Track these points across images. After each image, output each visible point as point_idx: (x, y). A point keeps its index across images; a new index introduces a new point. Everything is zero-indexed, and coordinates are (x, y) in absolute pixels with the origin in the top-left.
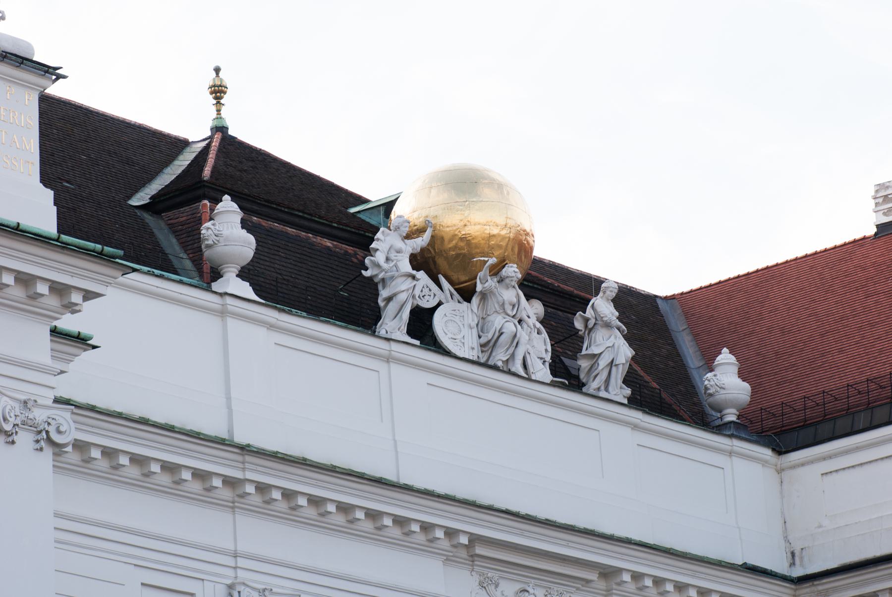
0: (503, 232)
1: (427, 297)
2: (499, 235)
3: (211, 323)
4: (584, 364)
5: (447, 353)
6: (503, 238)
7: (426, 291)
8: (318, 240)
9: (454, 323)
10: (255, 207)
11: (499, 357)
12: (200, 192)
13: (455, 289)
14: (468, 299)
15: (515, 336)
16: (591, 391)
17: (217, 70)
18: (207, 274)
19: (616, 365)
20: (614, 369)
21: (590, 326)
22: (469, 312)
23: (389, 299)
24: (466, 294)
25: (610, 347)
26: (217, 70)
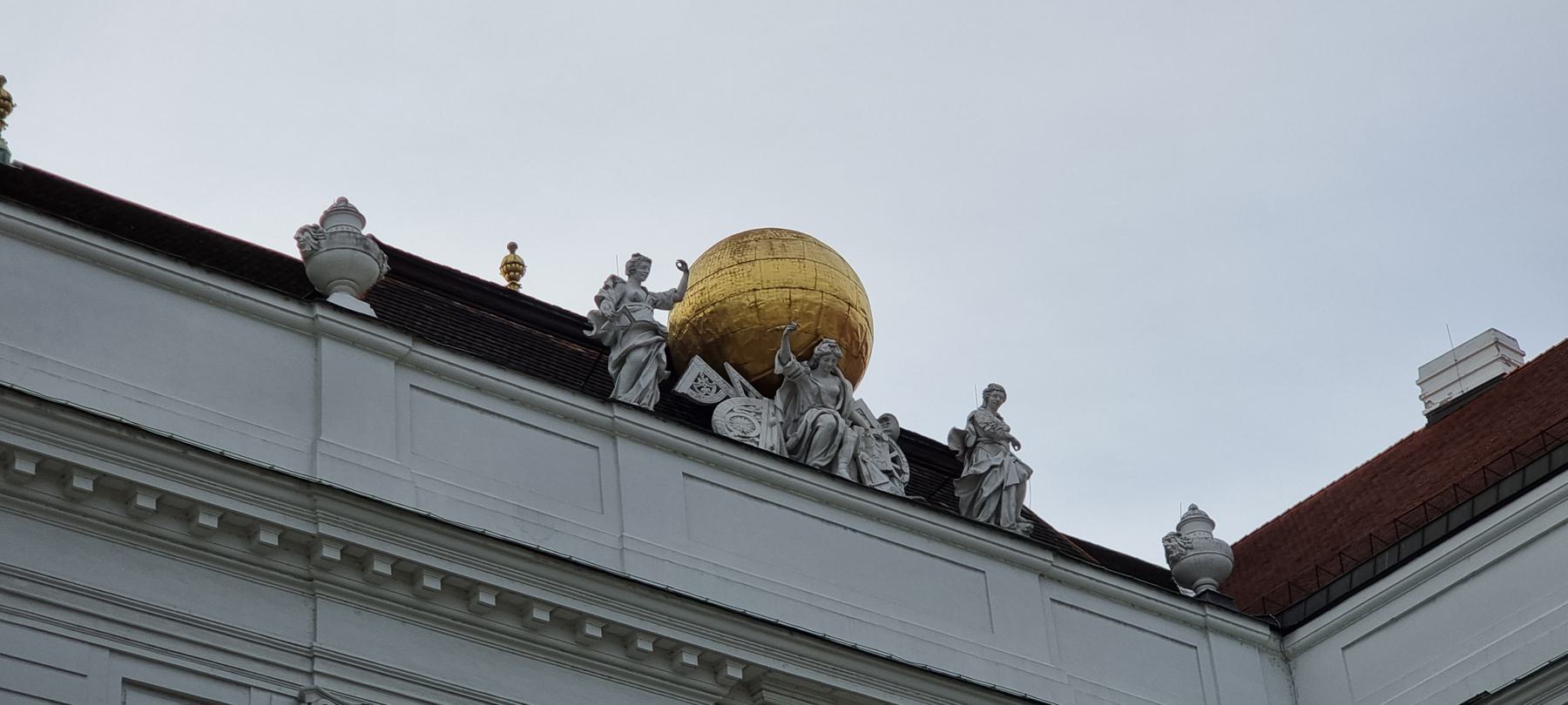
0: (812, 297)
1: (705, 390)
2: (805, 301)
3: (292, 349)
6: (812, 304)
8: (564, 343)
13: (752, 384)
14: (772, 396)
15: (836, 431)
17: (512, 247)
19: (1008, 488)
20: (1005, 494)
21: (970, 443)
23: (621, 362)
24: (766, 386)
26: (512, 247)
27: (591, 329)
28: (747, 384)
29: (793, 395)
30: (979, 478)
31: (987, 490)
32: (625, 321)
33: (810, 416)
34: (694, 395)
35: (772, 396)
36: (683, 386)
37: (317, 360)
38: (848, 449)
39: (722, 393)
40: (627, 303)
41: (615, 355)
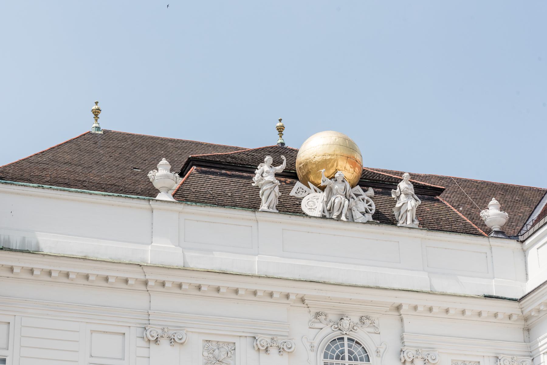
4: (396, 213)
5: (307, 215)
7: (300, 190)
9: (313, 202)
10: (222, 166)
11: (335, 215)
12: (191, 163)
14: (323, 191)
16: (399, 225)
18: (150, 192)
22: (322, 196)
23: (263, 194)
25: (406, 202)
27: (254, 183)
28: (316, 188)
29: (331, 190)
30: (400, 208)
31: (402, 211)
32: (262, 182)
33: (333, 199)
34: (296, 196)
35: (323, 191)
36: (292, 193)
37: (152, 217)
38: (345, 211)
39: (307, 193)
40: (264, 175)
41: (261, 192)
